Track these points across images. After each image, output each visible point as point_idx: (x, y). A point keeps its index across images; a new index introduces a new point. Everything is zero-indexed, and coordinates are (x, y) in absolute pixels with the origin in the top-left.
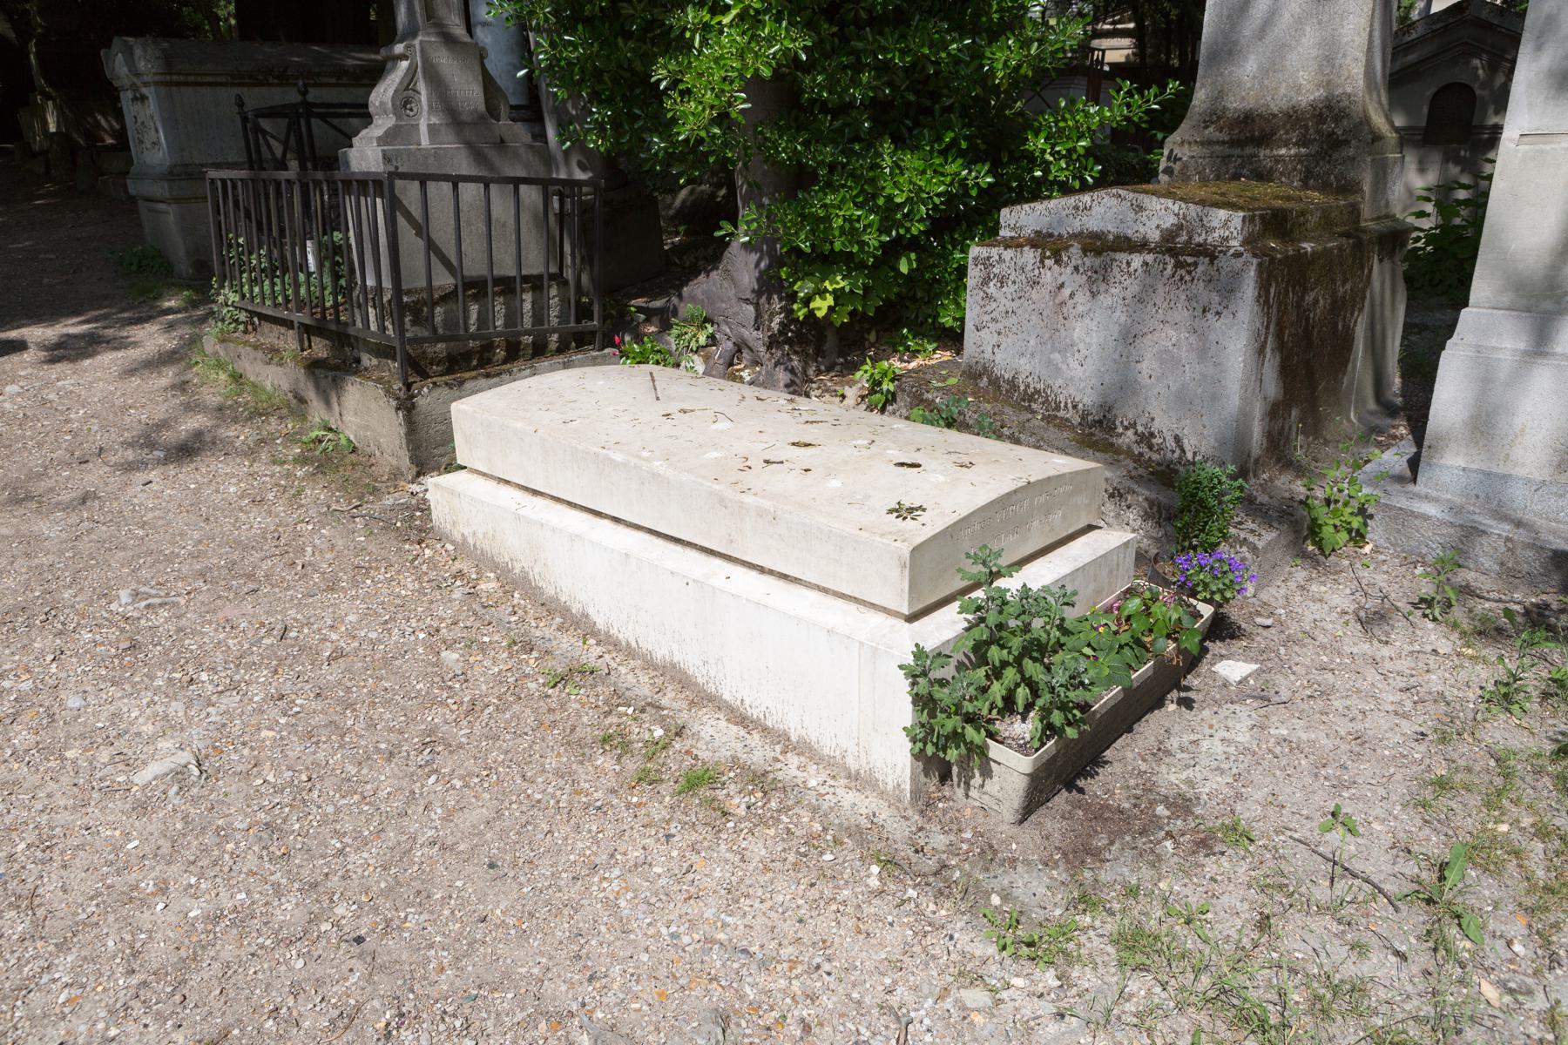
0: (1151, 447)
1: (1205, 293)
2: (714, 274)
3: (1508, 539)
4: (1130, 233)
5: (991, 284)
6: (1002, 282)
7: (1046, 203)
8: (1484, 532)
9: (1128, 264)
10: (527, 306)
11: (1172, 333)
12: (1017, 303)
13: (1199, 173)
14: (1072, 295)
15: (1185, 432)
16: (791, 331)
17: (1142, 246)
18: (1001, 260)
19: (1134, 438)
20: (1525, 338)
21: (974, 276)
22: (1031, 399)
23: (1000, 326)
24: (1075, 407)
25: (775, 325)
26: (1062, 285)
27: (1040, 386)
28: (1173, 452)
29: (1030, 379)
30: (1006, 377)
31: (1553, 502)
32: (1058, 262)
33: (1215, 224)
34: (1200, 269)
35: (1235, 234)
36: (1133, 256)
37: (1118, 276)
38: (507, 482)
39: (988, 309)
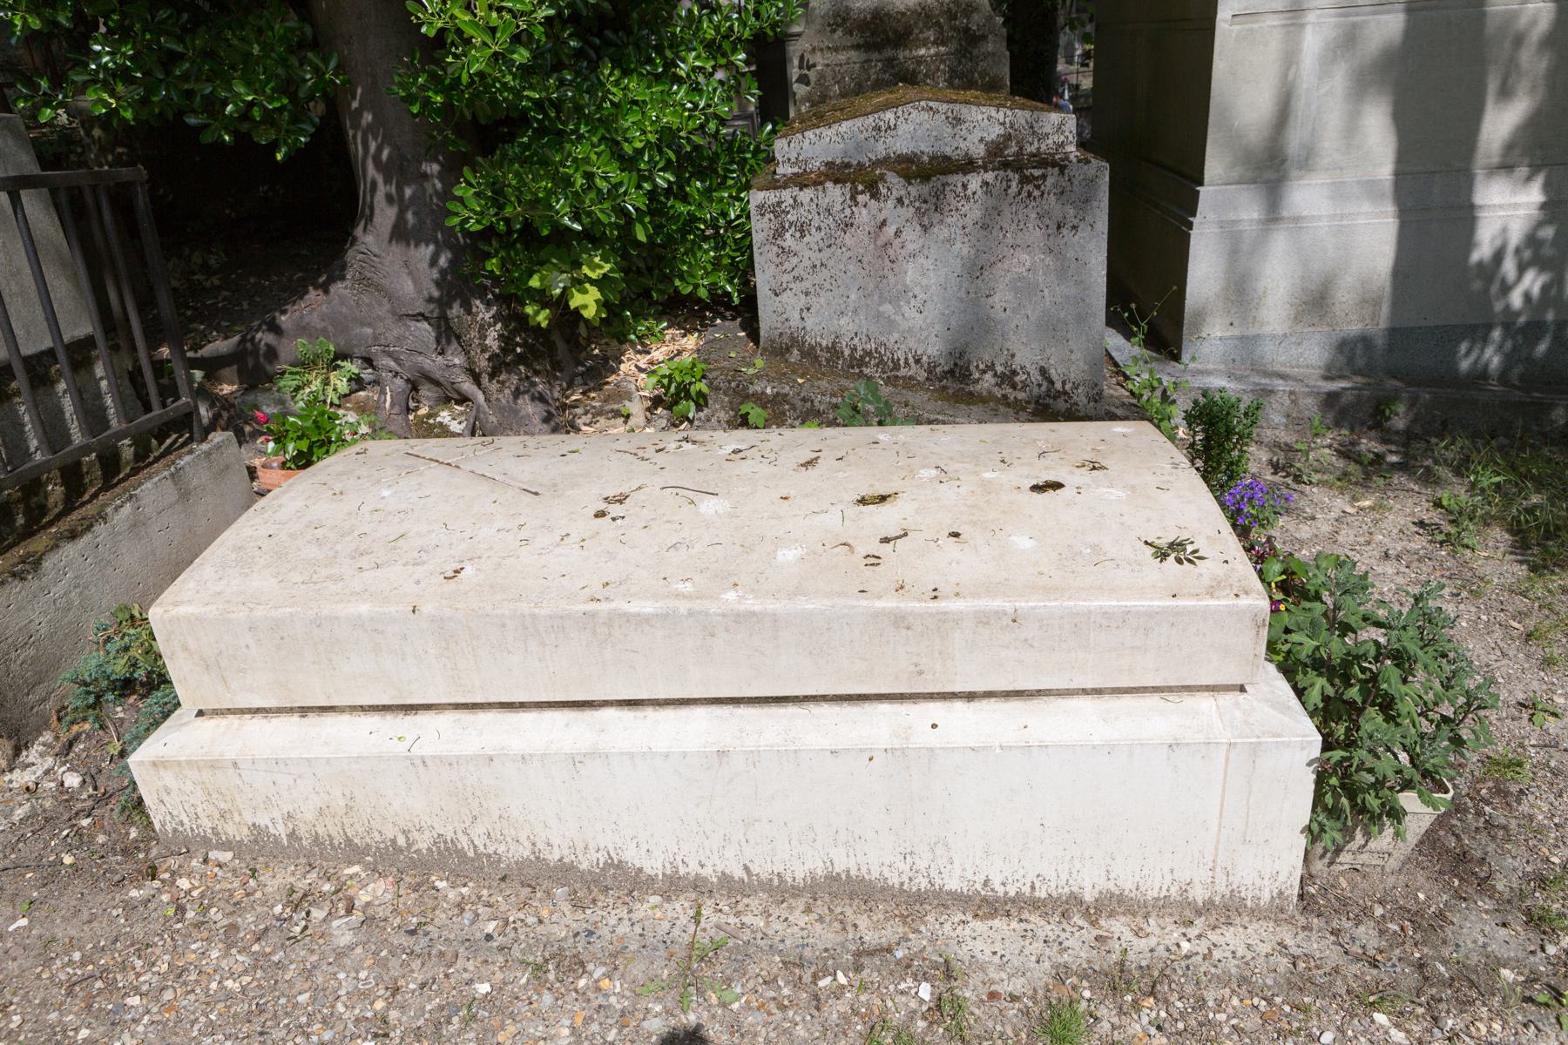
0: (1014, 387)
1: (1058, 207)
2: (338, 288)
3: (1292, 393)
4: (948, 151)
5: (788, 235)
6: (802, 230)
7: (835, 126)
8: (1272, 392)
9: (965, 186)
10: (68, 405)
11: (1025, 257)
12: (827, 253)
13: (838, 82)
14: (898, 233)
15: (1052, 361)
16: (518, 344)
17: (968, 165)
18: (796, 204)
19: (993, 381)
20: (1256, 208)
21: (760, 228)
22: (861, 363)
23: (807, 284)
24: (918, 361)
25: (492, 341)
26: (884, 223)
27: (871, 346)
28: (1040, 386)
29: (856, 341)
30: (824, 343)
31: (1294, 351)
32: (875, 195)
33: (1047, 129)
34: (1050, 181)
35: (1071, 138)
36: (969, 177)
37: (954, 202)
38: (331, 709)
39: (787, 266)
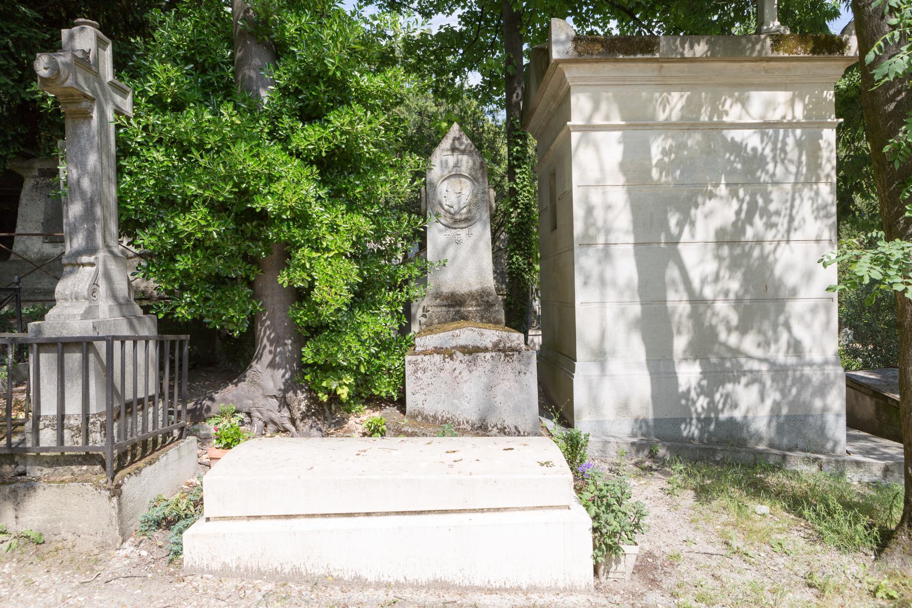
3: (617, 443)
4: (479, 345)
12: (434, 379)
14: (460, 373)
17: (486, 350)
19: (497, 431)
21: (409, 369)
23: (425, 391)
24: (467, 422)
25: (303, 407)
26: (455, 369)
29: (444, 414)
32: (452, 359)
33: (514, 339)
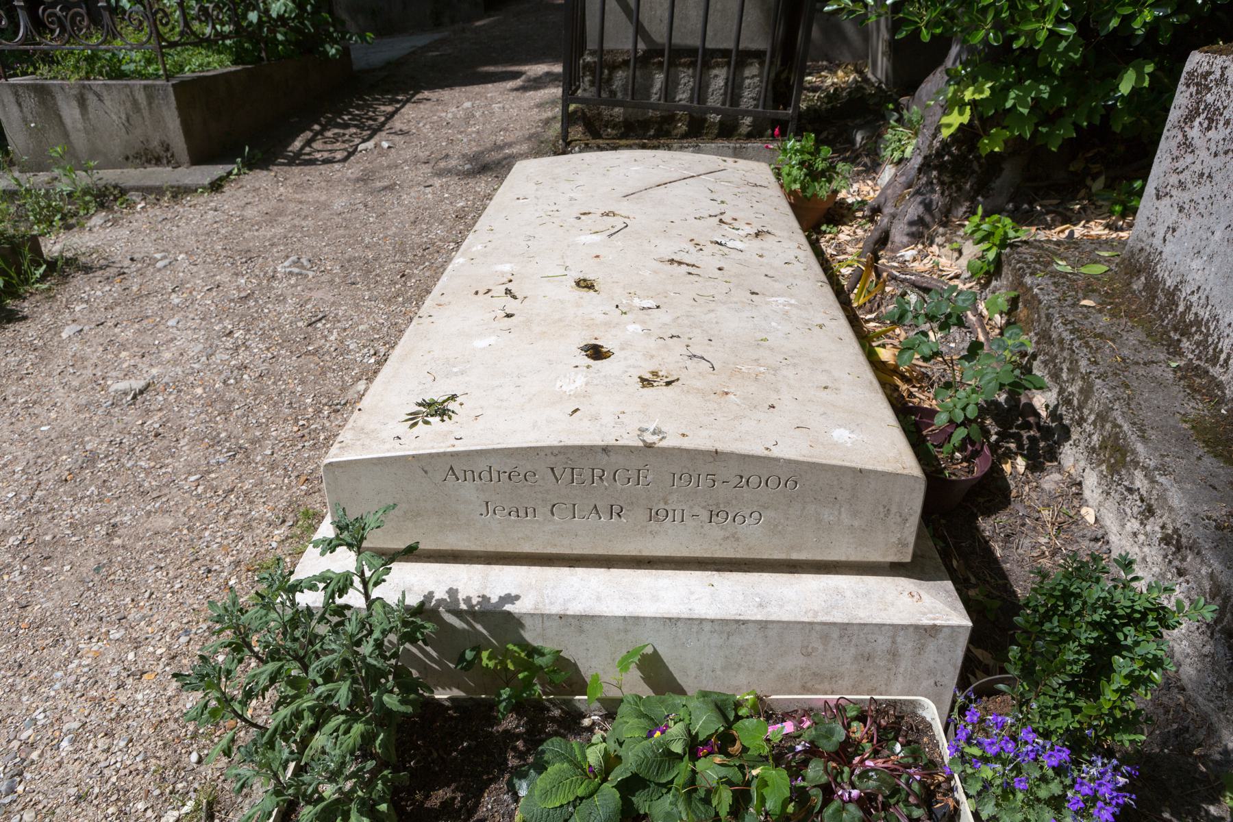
22: (1184, 329)
27: (1205, 314)
29: (1194, 298)
